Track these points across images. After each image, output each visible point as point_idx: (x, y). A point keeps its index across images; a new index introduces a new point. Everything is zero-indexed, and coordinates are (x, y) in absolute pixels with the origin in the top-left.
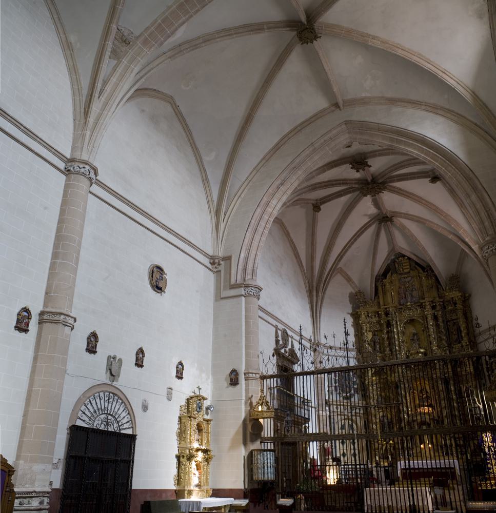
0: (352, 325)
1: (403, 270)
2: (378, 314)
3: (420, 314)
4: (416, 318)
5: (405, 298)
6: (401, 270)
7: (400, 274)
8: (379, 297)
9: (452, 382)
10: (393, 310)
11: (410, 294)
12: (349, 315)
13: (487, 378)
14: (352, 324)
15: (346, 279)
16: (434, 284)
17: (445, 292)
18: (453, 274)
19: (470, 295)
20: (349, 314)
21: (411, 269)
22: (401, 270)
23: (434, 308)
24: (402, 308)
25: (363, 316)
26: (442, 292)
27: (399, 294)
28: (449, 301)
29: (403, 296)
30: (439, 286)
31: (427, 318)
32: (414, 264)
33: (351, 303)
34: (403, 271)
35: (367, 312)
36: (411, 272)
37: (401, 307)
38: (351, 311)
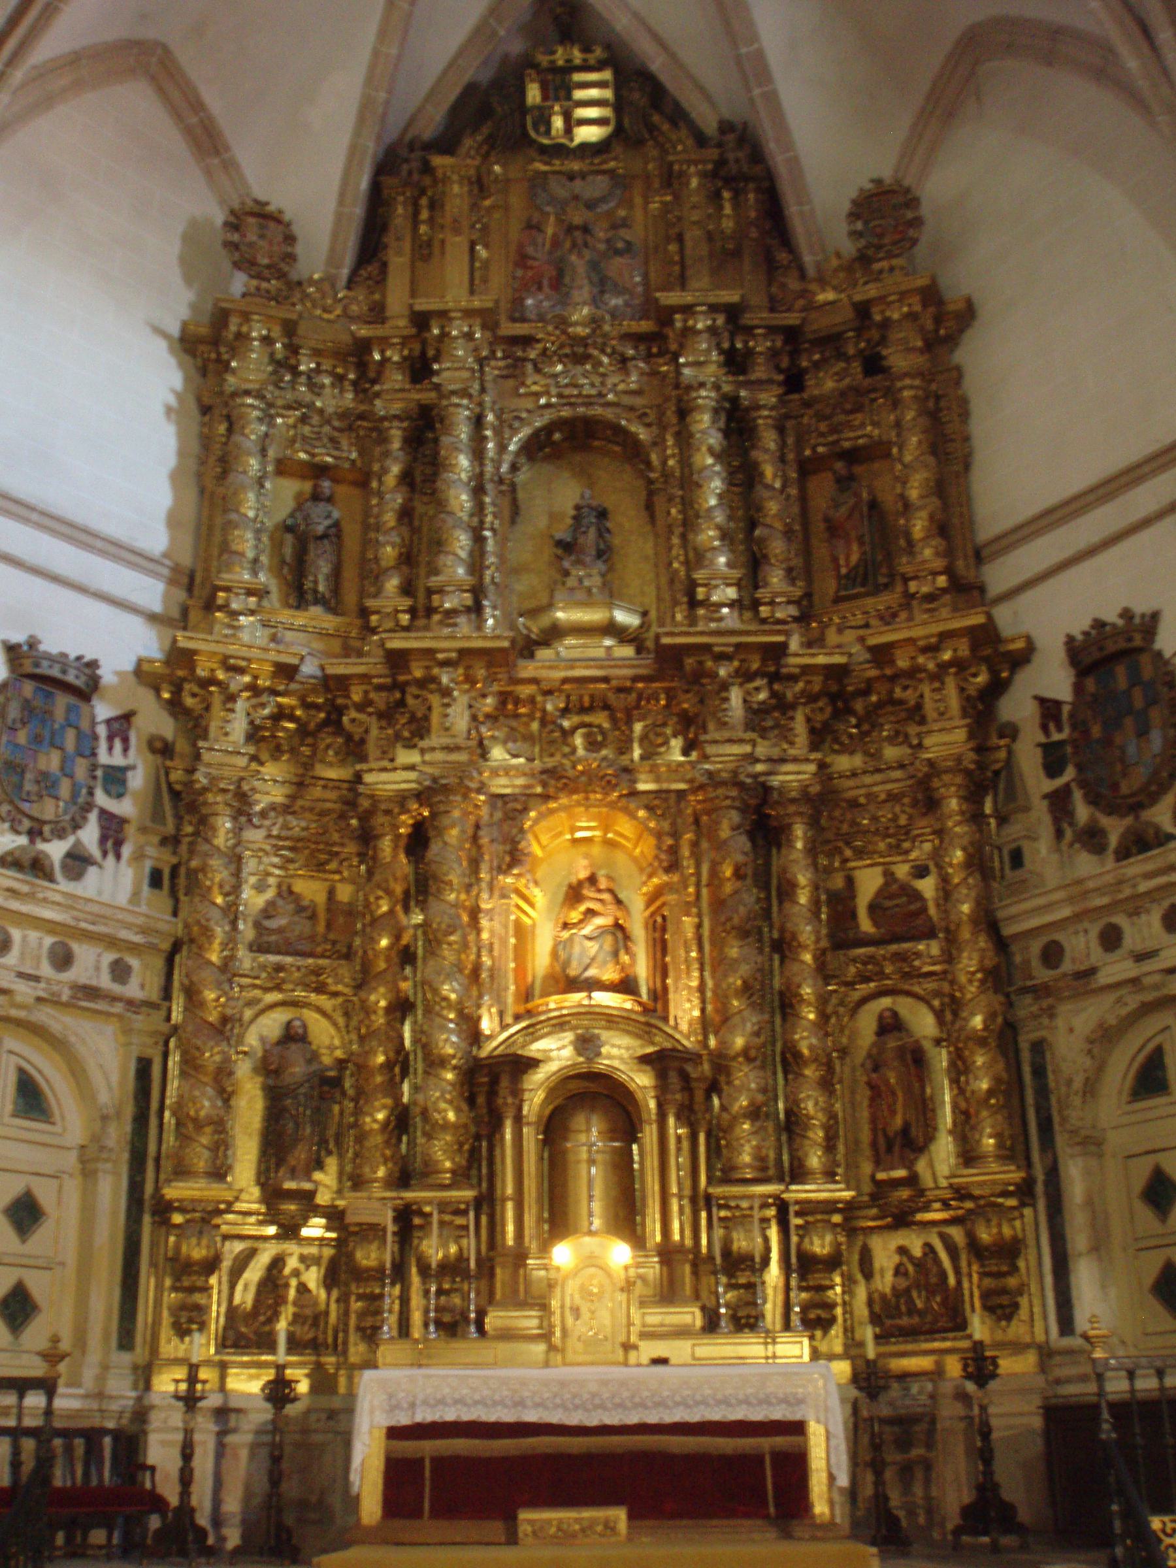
0: (169, 410)
1: (570, 124)
2: (362, 366)
3: (637, 393)
4: (609, 414)
5: (557, 283)
6: (558, 123)
7: (543, 150)
8: (385, 265)
9: (799, 835)
10: (469, 336)
11: (594, 266)
12: (163, 344)
13: (1040, 812)
14: (172, 400)
15: (188, 131)
16: (754, 233)
17: (813, 287)
18: (878, 182)
19: (968, 314)
20: (159, 331)
21: (619, 132)
22: (558, 123)
23: (735, 362)
24: (527, 341)
25: (256, 353)
26: (794, 285)
27: (522, 260)
28: (831, 341)
29: (550, 272)
30: (783, 256)
31: (683, 413)
32: (637, 97)
33: (188, 279)
34: (568, 131)
35: (290, 328)
36: (618, 149)
37: (520, 329)
38: (175, 330)
